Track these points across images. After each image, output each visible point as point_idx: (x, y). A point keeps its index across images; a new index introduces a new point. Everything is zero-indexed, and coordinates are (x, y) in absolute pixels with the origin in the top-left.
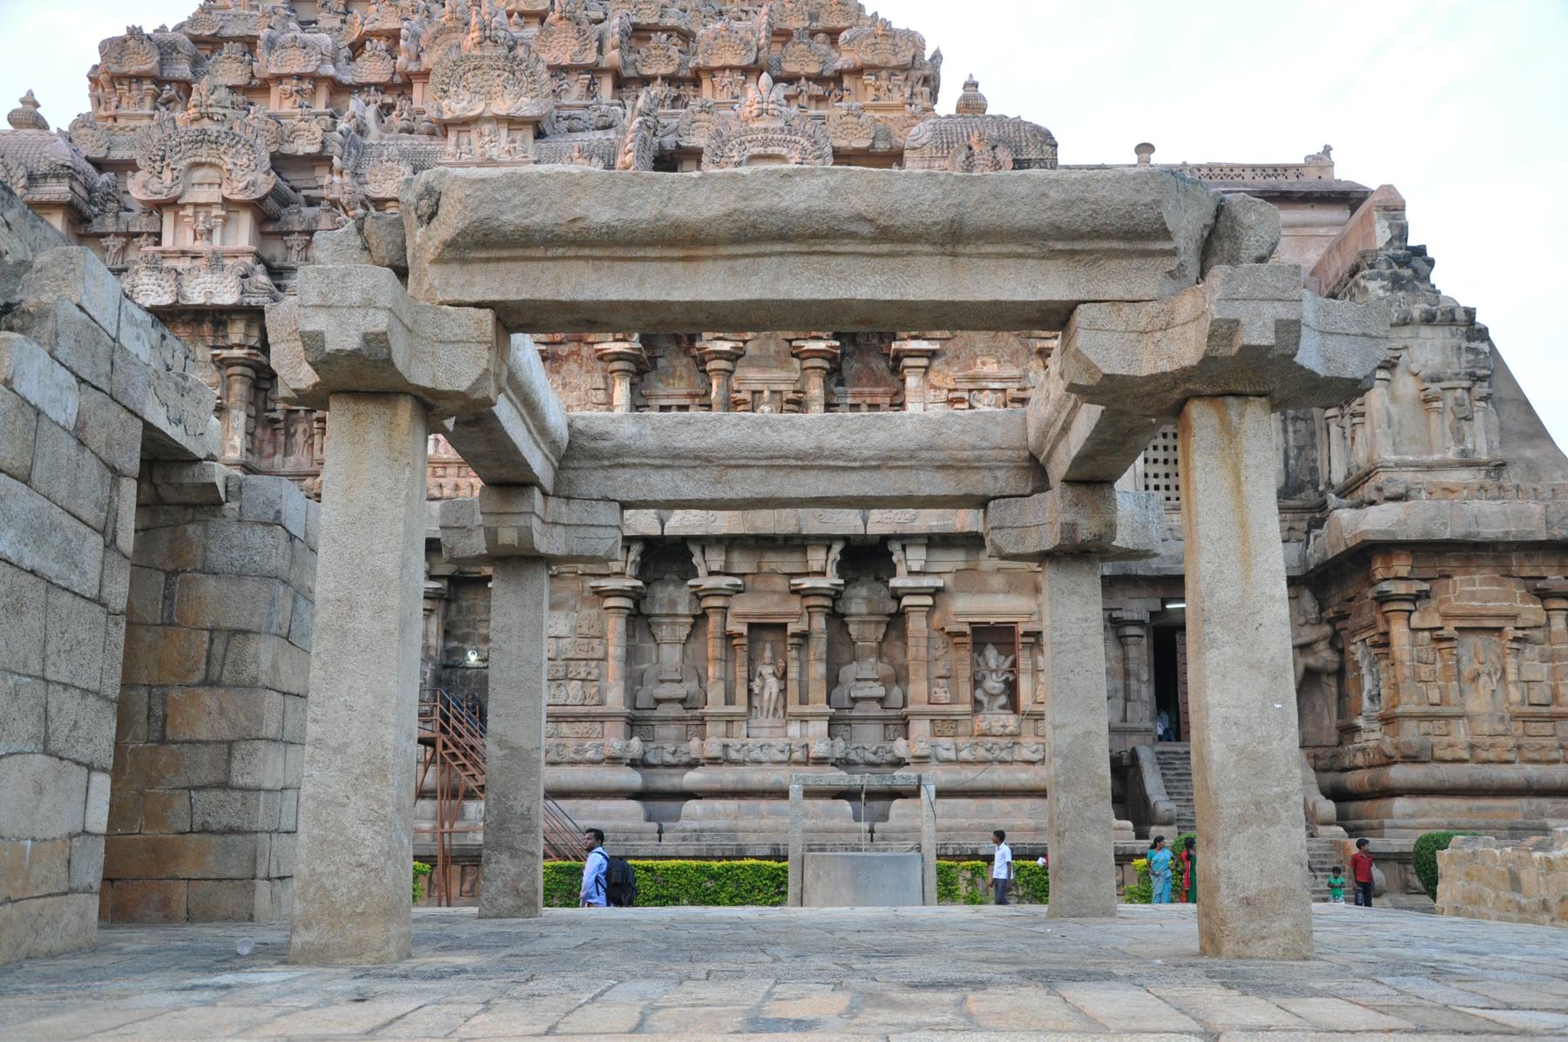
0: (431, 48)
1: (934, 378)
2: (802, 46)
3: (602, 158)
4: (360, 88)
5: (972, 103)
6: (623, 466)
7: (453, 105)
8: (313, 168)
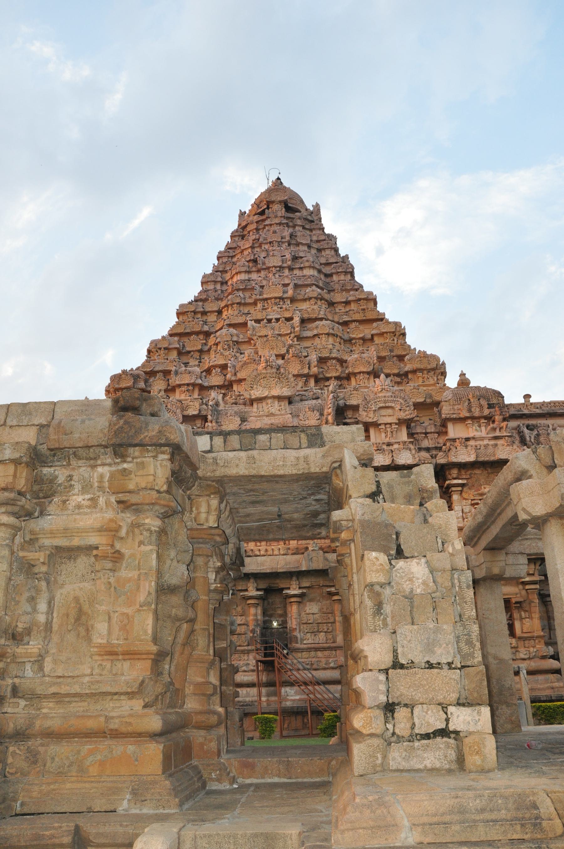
0: (241, 371)
1: (464, 495)
2: (390, 363)
3: (318, 411)
4: (211, 387)
5: (464, 382)
6: (527, 539)
7: (256, 393)
8: (195, 420)
